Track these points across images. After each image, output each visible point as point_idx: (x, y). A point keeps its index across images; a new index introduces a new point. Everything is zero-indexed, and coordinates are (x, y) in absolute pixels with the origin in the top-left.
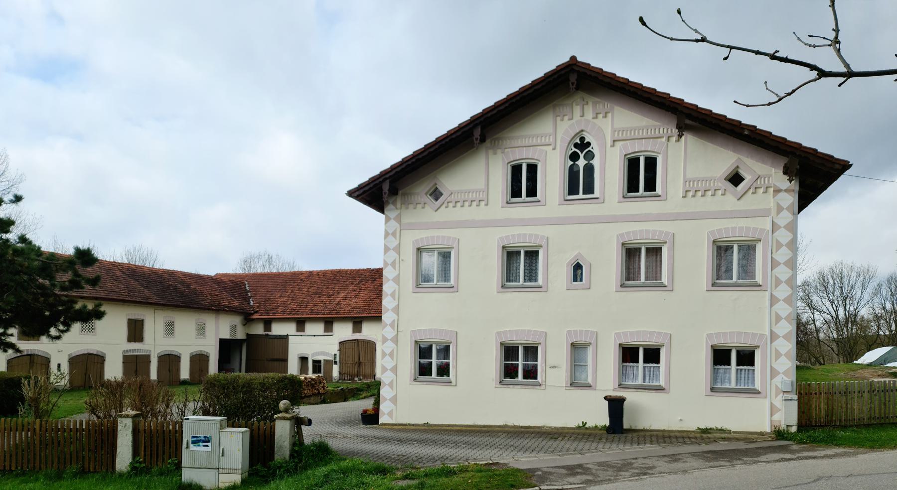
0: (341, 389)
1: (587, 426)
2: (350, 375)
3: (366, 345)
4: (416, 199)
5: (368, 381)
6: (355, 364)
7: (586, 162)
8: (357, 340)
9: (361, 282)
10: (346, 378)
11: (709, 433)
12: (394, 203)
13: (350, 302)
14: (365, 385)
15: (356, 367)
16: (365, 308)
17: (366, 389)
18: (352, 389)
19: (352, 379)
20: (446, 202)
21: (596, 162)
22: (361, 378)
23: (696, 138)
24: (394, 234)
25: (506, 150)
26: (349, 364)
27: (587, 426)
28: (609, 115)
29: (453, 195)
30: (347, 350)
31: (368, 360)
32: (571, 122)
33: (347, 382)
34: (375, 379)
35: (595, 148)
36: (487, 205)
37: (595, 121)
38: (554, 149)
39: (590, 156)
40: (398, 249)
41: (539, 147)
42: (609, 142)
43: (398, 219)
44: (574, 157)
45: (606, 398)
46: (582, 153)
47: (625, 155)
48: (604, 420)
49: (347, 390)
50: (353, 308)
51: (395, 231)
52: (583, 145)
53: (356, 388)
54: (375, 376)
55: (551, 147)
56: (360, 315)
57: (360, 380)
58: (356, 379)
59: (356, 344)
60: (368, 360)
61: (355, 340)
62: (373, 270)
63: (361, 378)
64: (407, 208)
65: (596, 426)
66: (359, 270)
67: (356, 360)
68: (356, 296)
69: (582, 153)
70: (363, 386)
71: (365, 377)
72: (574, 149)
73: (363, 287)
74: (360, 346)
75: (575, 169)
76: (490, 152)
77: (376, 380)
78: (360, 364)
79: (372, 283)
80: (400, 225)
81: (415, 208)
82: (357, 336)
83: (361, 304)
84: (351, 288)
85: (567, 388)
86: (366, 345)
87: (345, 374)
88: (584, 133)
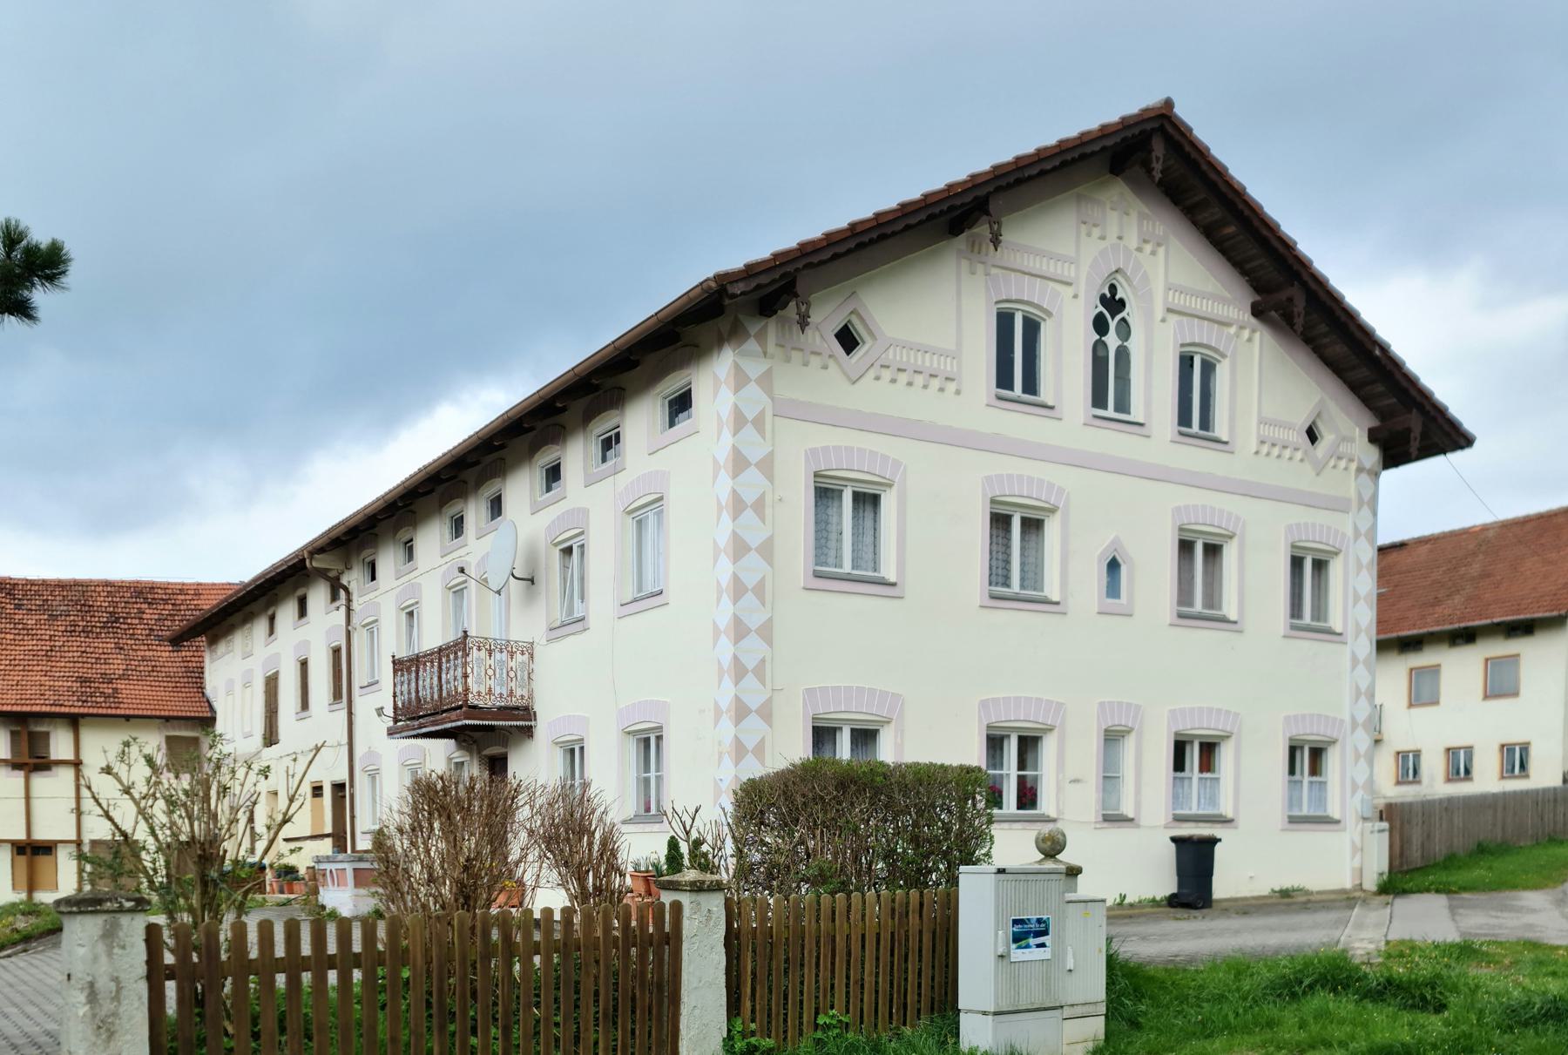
1: (1127, 901)
4: (810, 340)
7: (1120, 343)
12: (761, 337)
20: (877, 365)
21: (1135, 345)
24: (758, 423)
25: (994, 271)
27: (1127, 901)
28: (1161, 251)
29: (891, 351)
32: (1103, 244)
35: (1131, 313)
36: (958, 392)
37: (1138, 254)
38: (1075, 296)
39: (1125, 330)
40: (767, 466)
41: (1051, 284)
42: (1159, 312)
43: (766, 381)
44: (1100, 325)
45: (1174, 840)
46: (1113, 318)
47: (1182, 345)
48: (1166, 885)
51: (762, 413)
52: (1113, 303)
55: (1069, 291)
64: (788, 360)
65: (1140, 902)
69: (1113, 318)
72: (1101, 309)
75: (1101, 353)
76: (965, 264)
80: (773, 399)
81: (806, 364)
85: (1098, 826)
88: (1119, 277)
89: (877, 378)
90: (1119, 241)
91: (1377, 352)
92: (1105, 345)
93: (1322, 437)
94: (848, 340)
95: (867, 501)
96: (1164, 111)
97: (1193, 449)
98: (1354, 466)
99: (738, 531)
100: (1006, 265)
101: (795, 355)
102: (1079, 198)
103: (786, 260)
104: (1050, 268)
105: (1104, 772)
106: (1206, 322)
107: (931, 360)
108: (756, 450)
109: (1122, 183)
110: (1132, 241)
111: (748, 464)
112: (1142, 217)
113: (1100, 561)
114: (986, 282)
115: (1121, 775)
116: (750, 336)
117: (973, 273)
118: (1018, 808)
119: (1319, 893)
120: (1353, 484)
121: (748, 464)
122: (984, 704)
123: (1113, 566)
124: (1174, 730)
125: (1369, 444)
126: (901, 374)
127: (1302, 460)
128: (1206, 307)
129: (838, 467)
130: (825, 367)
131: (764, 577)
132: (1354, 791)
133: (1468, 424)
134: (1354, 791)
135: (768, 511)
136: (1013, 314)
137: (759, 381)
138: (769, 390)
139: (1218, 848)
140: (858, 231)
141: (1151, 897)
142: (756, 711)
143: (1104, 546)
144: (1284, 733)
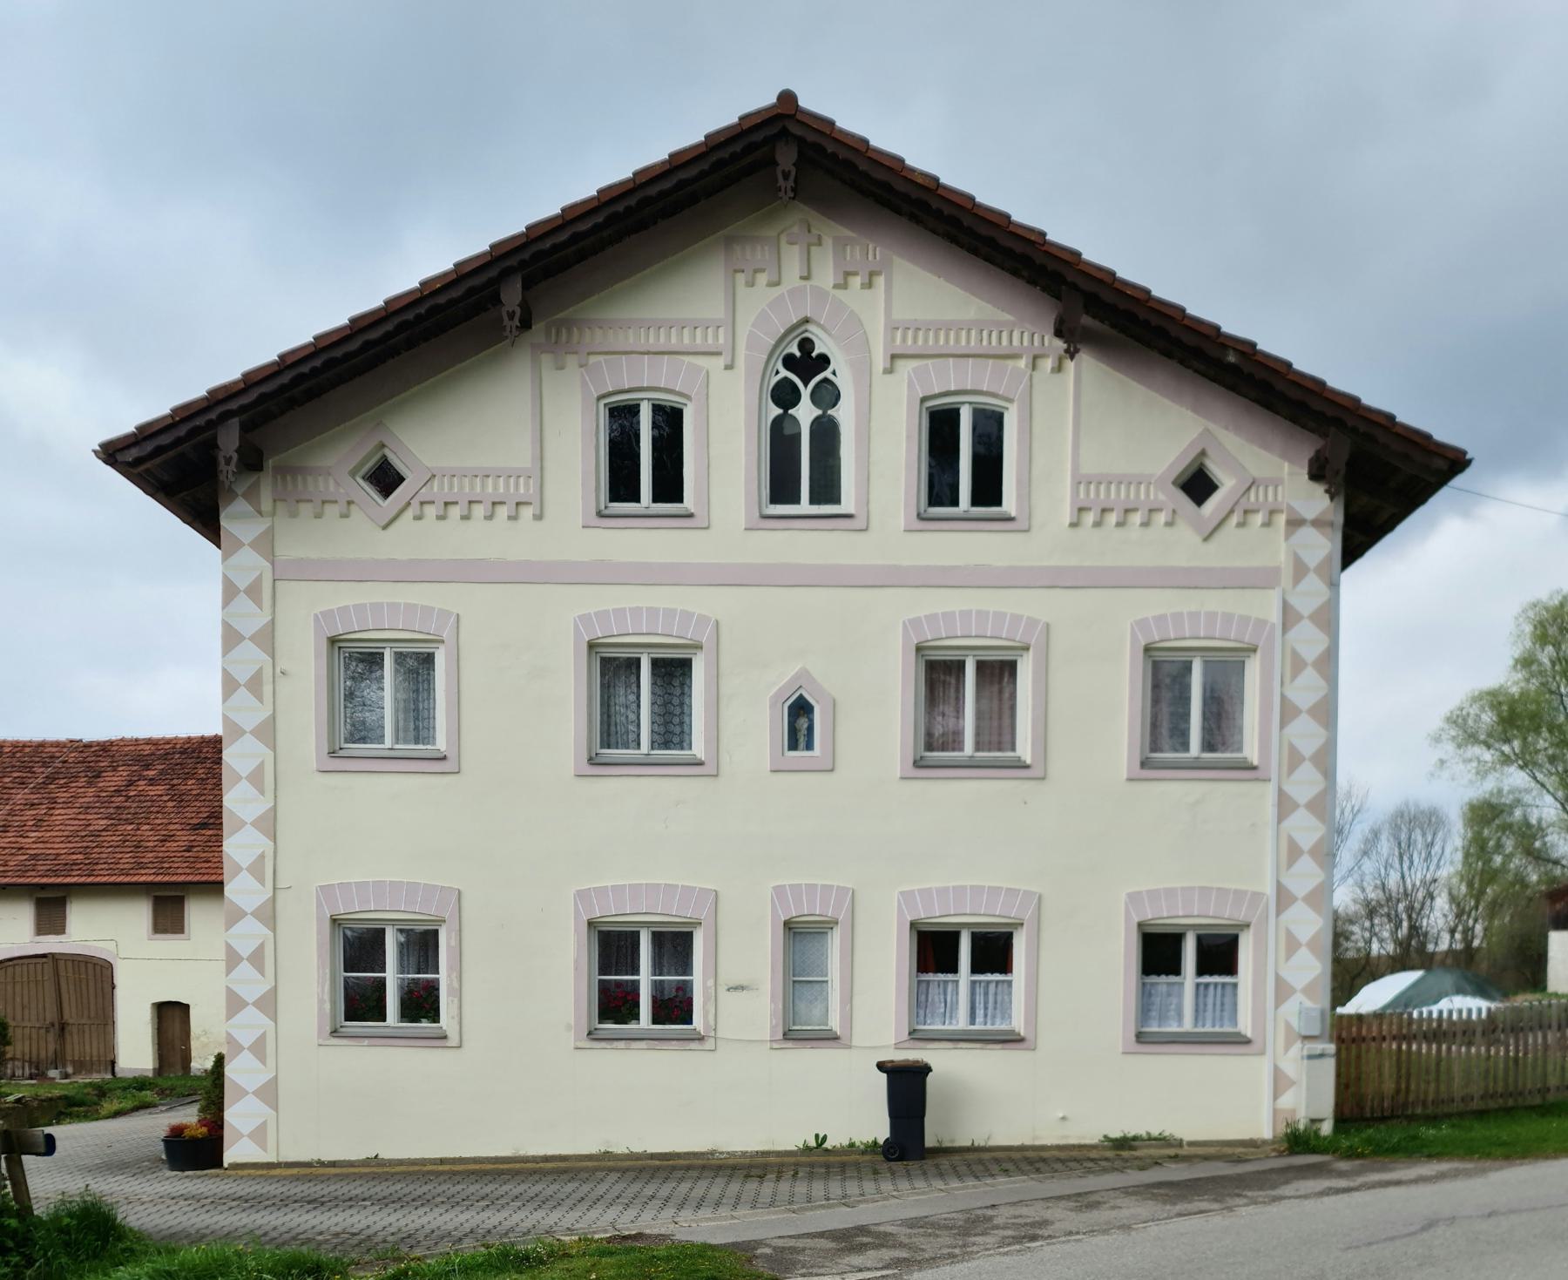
0: (18, 1101)
1: (827, 1145)
2: (30, 1062)
3: (83, 969)
4: (321, 486)
5: (96, 1078)
6: (47, 1031)
7: (819, 412)
8: (53, 955)
9: (51, 779)
10: (19, 1072)
11: (1132, 1148)
12: (252, 495)
13: (19, 839)
14: (89, 1090)
15: (51, 1037)
16: (74, 857)
17: (95, 1098)
18: (51, 1099)
19: (37, 1075)
20: (415, 503)
21: (844, 414)
22: (70, 1070)
23: (1104, 366)
24: (254, 591)
25: (593, 359)
26: (27, 1031)
27: (827, 1145)
28: (880, 281)
29: (436, 483)
30: (18, 987)
31: (89, 1017)
32: (776, 292)
33: (22, 1082)
34: (113, 1073)
35: (841, 372)
36: (539, 517)
37: (839, 293)
38: (729, 367)
39: (828, 395)
40: (267, 639)
41: (687, 359)
42: (880, 361)
43: (266, 545)
44: (785, 396)
45: (881, 1066)
46: (806, 385)
47: (923, 400)
48: (878, 1128)
49: (35, 1104)
50: (34, 857)
51: (259, 580)
52: (808, 362)
53: (66, 1098)
54: (113, 1063)
55: (720, 362)
56: (59, 880)
57: (66, 1076)
58: (53, 1073)
59: (48, 968)
60: (89, 1017)
61: (44, 956)
62: (89, 745)
63: (70, 1070)
64: (294, 515)
65: (852, 1145)
66: (42, 745)
67: (51, 1015)
68: (39, 823)
69: (806, 385)
70: (86, 1091)
71: (81, 1066)
72: (784, 373)
73: (63, 796)
74: (62, 973)
75: (788, 431)
76: (546, 359)
77: (119, 1075)
78: (63, 1027)
79: (90, 784)
80: (273, 564)
81: (318, 516)
82: (51, 944)
83: (61, 848)
84: (20, 796)
85: (775, 1046)
86: (83, 969)
87: (13, 1059)
88: (810, 327)
89: (418, 518)
90: (803, 283)
91: (1232, 358)
92: (795, 420)
93: (1222, 484)
94: (385, 479)
95: (418, 667)
96: (779, 111)
97: (993, 536)
98: (1281, 520)
99: (229, 715)
100: (611, 350)
101: (305, 508)
102: (729, 242)
103: (187, 414)
104: (653, 340)
105: (602, 971)
106: (951, 360)
107: (483, 486)
108: (252, 619)
109: (802, 206)
110: (825, 275)
111: (241, 638)
112: (840, 244)
113: (772, 706)
114: (583, 375)
115: (829, 978)
116: (237, 495)
117: (562, 368)
118: (655, 1021)
119: (1192, 1144)
120: (1283, 546)
121: (241, 638)
122: (582, 895)
123: (800, 709)
124: (1136, 920)
125: (1311, 483)
126: (475, 507)
127: (1169, 524)
128: (991, 342)
129: (368, 630)
130: (345, 516)
131: (263, 762)
132: (1280, 999)
133: (1443, 432)
134: (1280, 999)
135: (267, 689)
136: (638, 406)
137: (254, 545)
138: (271, 556)
139: (930, 1078)
140: (289, 362)
141: (871, 1140)
142: (251, 914)
143: (781, 685)
144: (1127, 912)
